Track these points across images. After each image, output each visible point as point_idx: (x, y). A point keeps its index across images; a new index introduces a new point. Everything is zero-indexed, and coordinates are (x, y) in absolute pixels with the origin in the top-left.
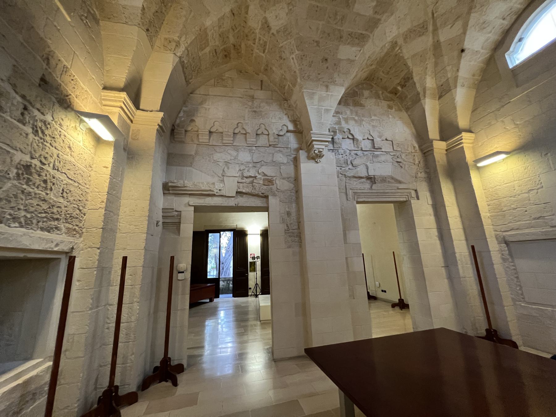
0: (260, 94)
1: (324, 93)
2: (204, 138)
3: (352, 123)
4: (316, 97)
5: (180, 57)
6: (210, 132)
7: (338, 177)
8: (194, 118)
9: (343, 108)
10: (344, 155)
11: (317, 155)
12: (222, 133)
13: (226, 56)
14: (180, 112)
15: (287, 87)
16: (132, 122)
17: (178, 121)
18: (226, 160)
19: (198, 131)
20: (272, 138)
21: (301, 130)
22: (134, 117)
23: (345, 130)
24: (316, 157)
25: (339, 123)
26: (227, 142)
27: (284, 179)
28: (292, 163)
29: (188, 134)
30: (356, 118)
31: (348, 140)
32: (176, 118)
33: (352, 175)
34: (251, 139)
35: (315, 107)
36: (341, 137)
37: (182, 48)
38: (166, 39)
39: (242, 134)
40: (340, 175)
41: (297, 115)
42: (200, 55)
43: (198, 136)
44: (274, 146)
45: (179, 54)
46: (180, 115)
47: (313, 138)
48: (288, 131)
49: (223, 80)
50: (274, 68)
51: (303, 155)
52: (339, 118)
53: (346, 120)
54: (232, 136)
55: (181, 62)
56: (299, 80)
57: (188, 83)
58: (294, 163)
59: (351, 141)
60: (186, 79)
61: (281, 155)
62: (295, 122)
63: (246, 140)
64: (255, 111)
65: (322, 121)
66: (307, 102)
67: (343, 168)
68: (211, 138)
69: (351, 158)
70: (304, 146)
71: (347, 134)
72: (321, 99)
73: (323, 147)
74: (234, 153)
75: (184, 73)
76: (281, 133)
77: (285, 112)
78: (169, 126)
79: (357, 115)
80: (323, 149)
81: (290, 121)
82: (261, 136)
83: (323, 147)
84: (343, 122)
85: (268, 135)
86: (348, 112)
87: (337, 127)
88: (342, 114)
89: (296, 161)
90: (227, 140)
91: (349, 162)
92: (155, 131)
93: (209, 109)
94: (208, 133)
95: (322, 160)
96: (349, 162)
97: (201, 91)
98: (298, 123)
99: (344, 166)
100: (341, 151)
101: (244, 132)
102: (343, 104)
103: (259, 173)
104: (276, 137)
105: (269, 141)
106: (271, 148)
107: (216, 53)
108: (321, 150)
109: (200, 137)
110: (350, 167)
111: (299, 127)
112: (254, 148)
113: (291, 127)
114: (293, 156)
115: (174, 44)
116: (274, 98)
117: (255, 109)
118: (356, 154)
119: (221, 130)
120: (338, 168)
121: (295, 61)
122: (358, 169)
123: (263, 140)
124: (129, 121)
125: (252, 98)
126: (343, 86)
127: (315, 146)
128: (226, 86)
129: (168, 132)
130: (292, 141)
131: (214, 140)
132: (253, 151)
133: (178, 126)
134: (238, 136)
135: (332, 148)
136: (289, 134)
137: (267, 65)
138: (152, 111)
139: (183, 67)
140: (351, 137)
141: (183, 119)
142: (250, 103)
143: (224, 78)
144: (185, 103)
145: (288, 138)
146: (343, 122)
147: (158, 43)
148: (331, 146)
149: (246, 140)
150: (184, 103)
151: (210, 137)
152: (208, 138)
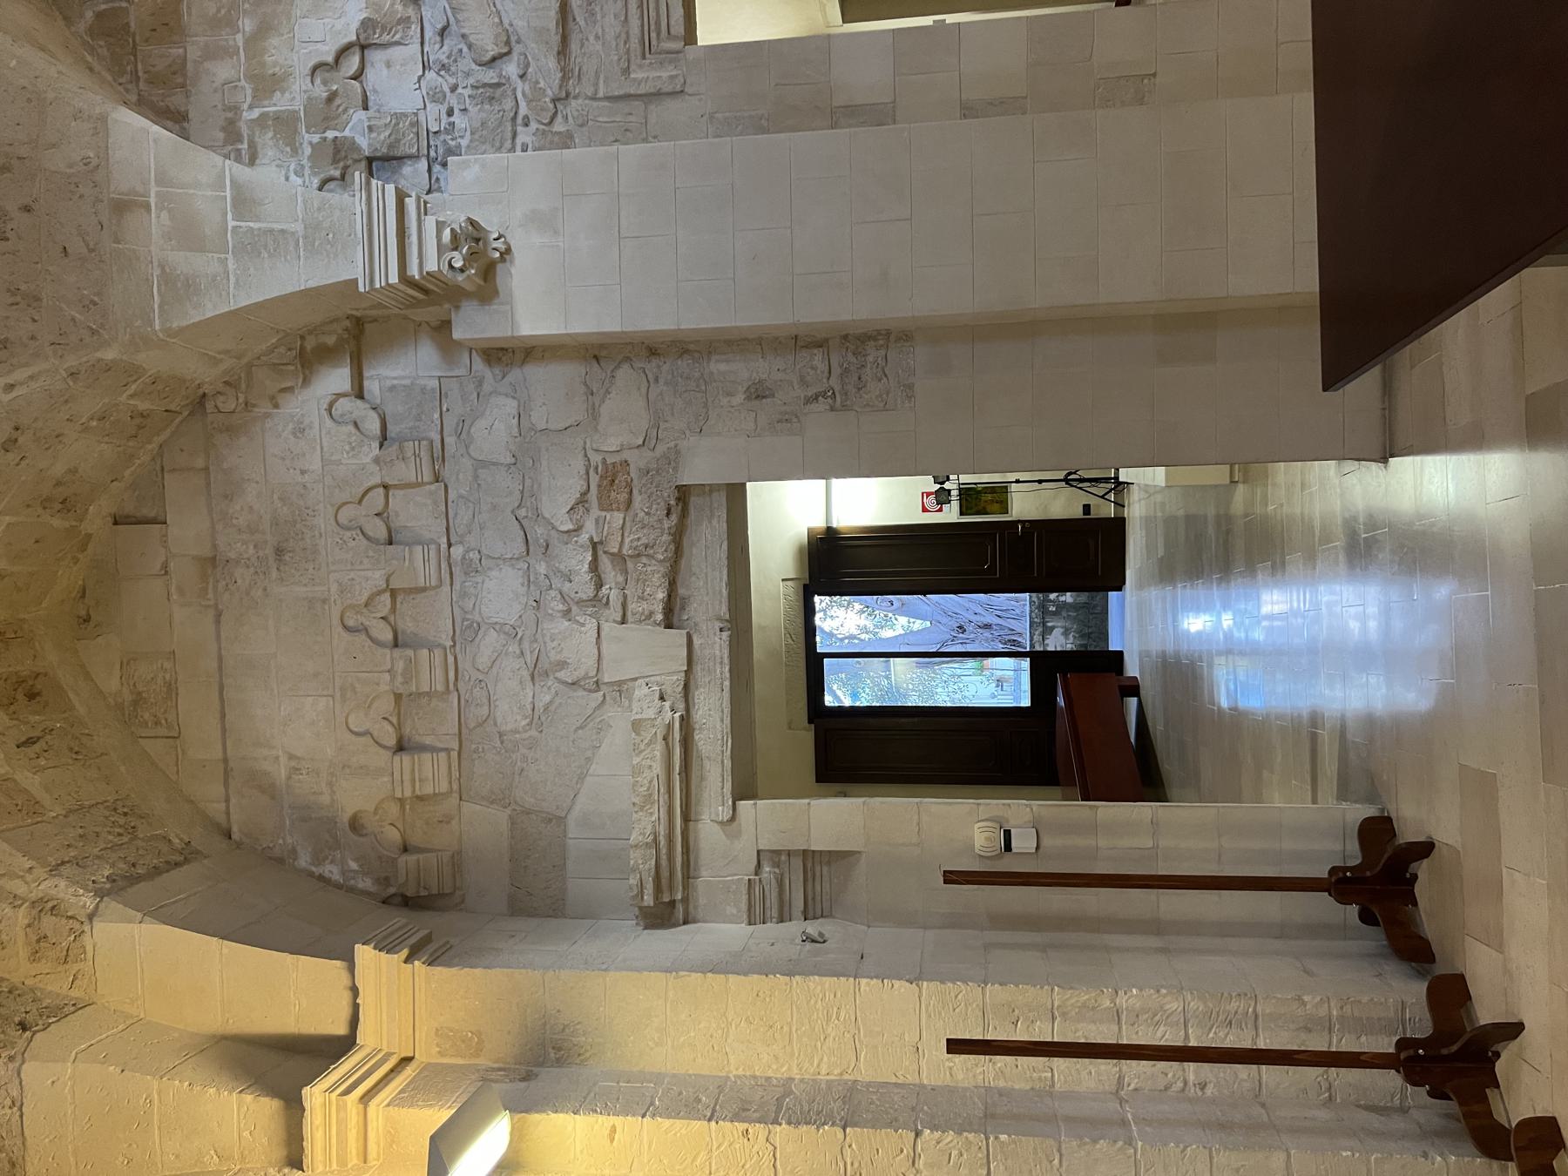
0: (187, 529)
1: (158, 222)
2: (432, 773)
3: (277, 54)
4: (185, 262)
5: (101, 894)
6: (400, 748)
7: (566, 141)
8: (346, 817)
9: (203, 103)
10: (452, 100)
11: (472, 256)
12: (398, 697)
13: (32, 696)
14: (321, 878)
15: (143, 406)
16: (407, 1060)
17: (366, 884)
18: (526, 674)
19: (401, 801)
20: (405, 472)
21: (347, 332)
22: (389, 1055)
23: (320, 92)
24: (483, 262)
25: (285, 125)
26: (439, 673)
27: (594, 414)
28: (515, 374)
29: (416, 839)
30: (247, 25)
31: (370, 74)
32: (351, 890)
33: (552, 63)
34: (419, 566)
35: (231, 265)
36: (362, 114)
37: (60, 888)
38: (35, 956)
39: (393, 609)
40: (559, 126)
41: (271, 350)
42: (59, 810)
43: (420, 798)
44: (439, 457)
45: (89, 902)
46: (336, 876)
47: (394, 279)
48: (360, 394)
49: (139, 700)
50: (59, 469)
51: (471, 325)
52: (262, 121)
53: (267, 84)
54: (410, 652)
55: (118, 887)
56: (109, 355)
57: (188, 855)
58: (511, 364)
59: (376, 56)
60: (177, 865)
61: (479, 428)
62: (308, 358)
63: (424, 589)
64: (279, 552)
65: (298, 227)
66: (212, 307)
67: (523, 110)
68: (428, 741)
69: (467, 63)
70: (431, 314)
71: (340, 79)
72: (188, 235)
73: (430, 223)
74: (490, 642)
75: (156, 872)
76: (373, 425)
77: (264, 407)
78: (398, 919)
79: (231, 24)
80: (440, 226)
81: (306, 382)
82: (398, 522)
83: (430, 223)
84: (280, 103)
85: (386, 487)
86: (223, 71)
87: (308, 138)
88: (236, 109)
89: (505, 355)
90: (430, 675)
91: (490, 76)
92: (438, 971)
93: (291, 757)
94: (406, 758)
95: (492, 226)
96: (490, 76)
97: (210, 794)
98: (310, 344)
99: (508, 104)
100: (433, 117)
101: (386, 597)
102: (176, 101)
103: (578, 530)
104: (392, 450)
105: (423, 484)
106: (446, 473)
107: (30, 742)
108: (447, 233)
109: (428, 790)
110: (511, 69)
111: (331, 340)
112: (457, 551)
113: (337, 378)
114: (477, 359)
115: (48, 922)
116: (200, 462)
117: (269, 551)
118: (443, 32)
119: (386, 705)
120: (524, 136)
121: (19, 375)
122: (520, 24)
123: (416, 512)
124: (409, 1072)
125: (212, 563)
126: (103, 119)
127: (432, 265)
128: (171, 689)
129: (425, 922)
130: (405, 369)
131: (436, 726)
132: (474, 555)
133: (385, 881)
134: (407, 626)
135: (423, 164)
136: (372, 387)
137: (46, 503)
138: (355, 991)
139: (134, 880)
140: (353, 62)
141: (354, 865)
142: (242, 575)
143: (128, 697)
144: (279, 861)
145: (392, 388)
146: (280, 103)
147: (56, 985)
148: (414, 173)
149: (424, 589)
150: (280, 861)
151: (423, 748)
152: (427, 756)
